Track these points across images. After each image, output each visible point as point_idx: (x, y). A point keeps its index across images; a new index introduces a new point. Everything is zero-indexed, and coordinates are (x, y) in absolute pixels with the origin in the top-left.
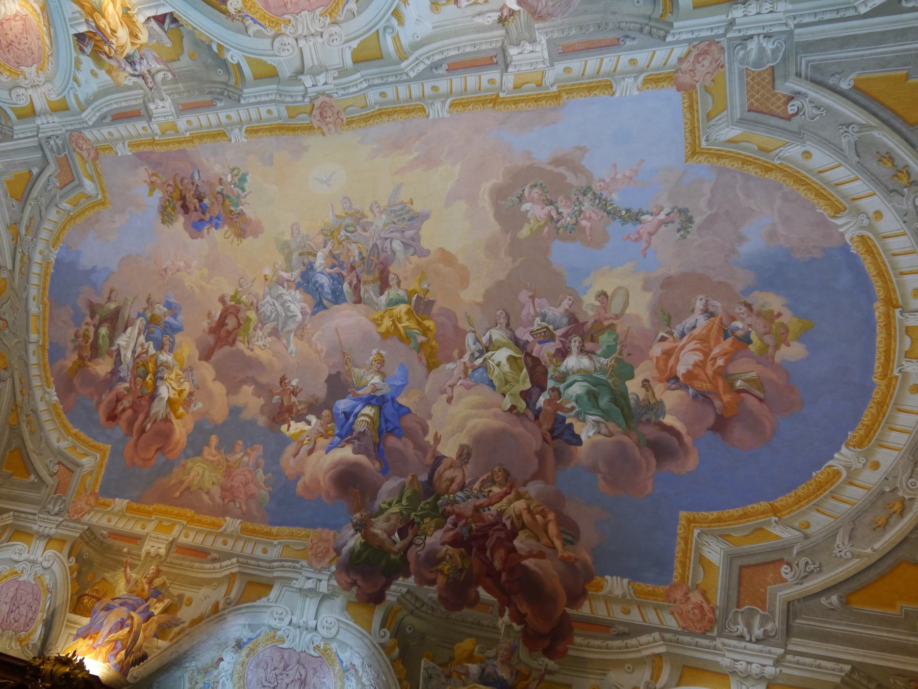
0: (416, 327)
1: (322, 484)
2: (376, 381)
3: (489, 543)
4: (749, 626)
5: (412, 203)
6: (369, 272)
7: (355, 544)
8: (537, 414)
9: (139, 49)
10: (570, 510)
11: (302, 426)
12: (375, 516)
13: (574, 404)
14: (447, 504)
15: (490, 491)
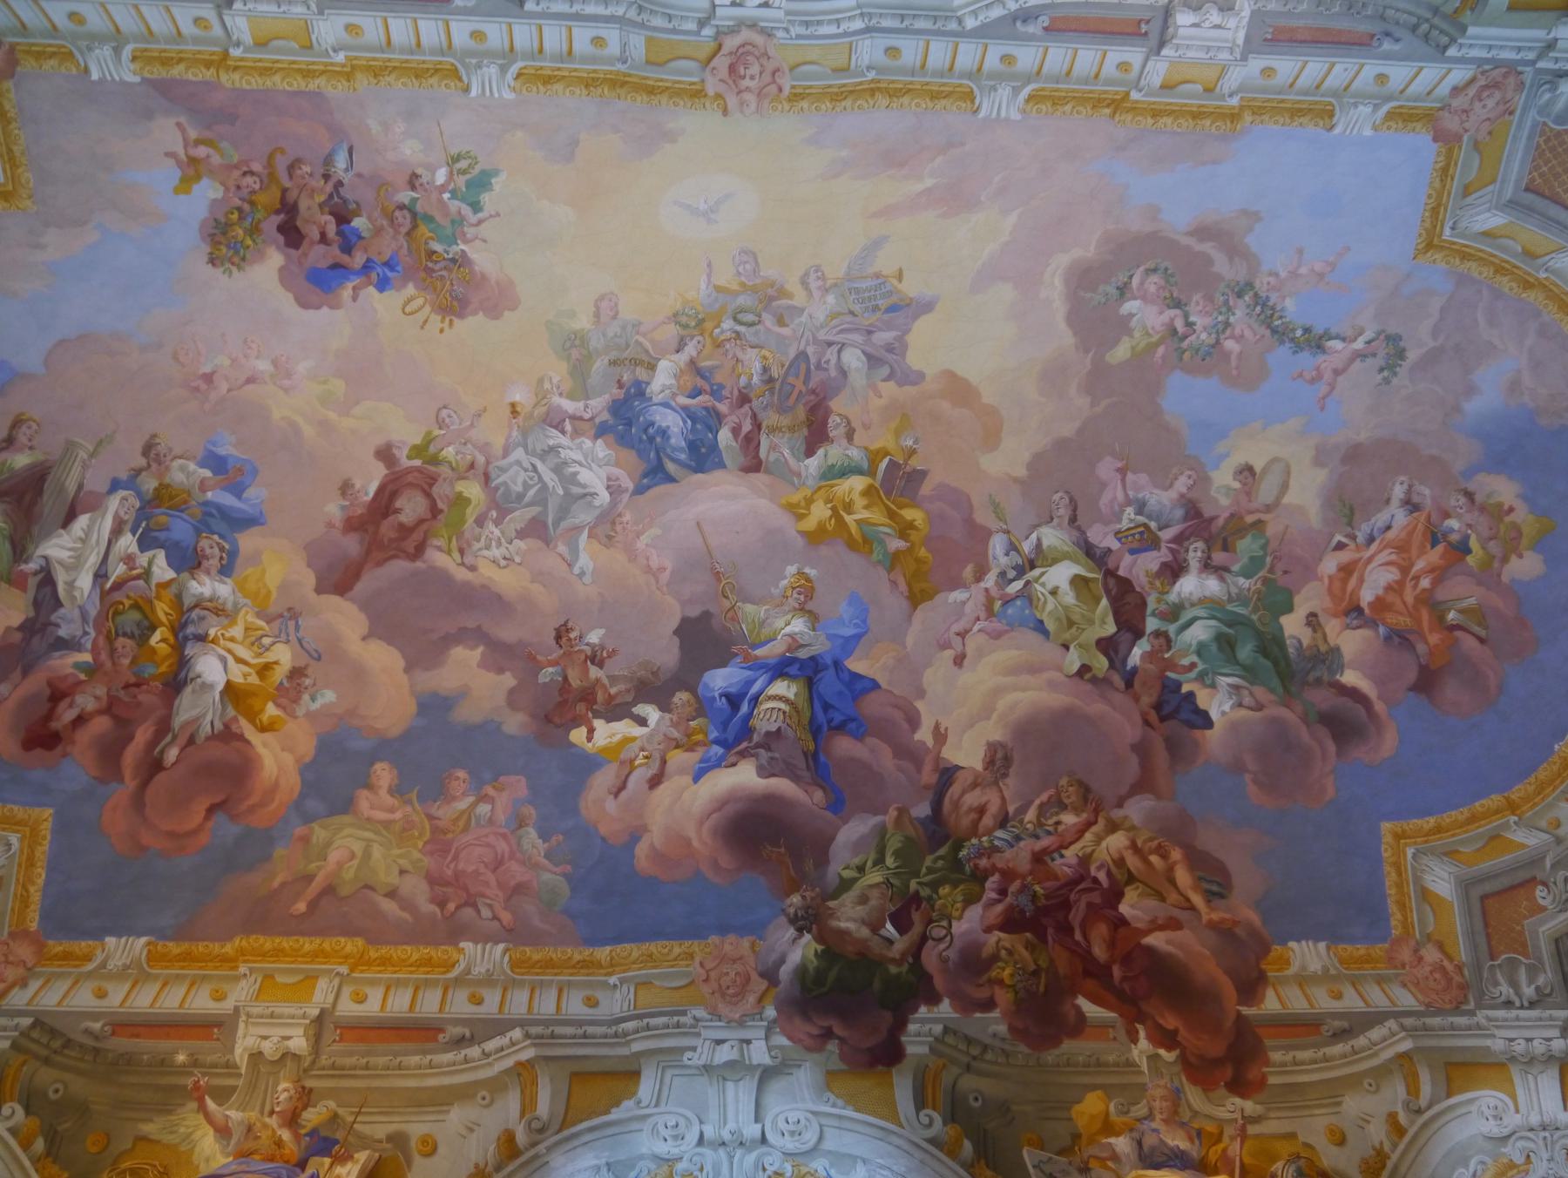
1: (695, 843)
2: (797, 630)
3: (1076, 916)
4: (1514, 984)
5: (900, 277)
6: (782, 410)
7: (804, 957)
8: (1130, 678)
10: (1207, 840)
11: (624, 728)
12: (835, 896)
13: (1195, 658)
14: (980, 855)
15: (1058, 823)
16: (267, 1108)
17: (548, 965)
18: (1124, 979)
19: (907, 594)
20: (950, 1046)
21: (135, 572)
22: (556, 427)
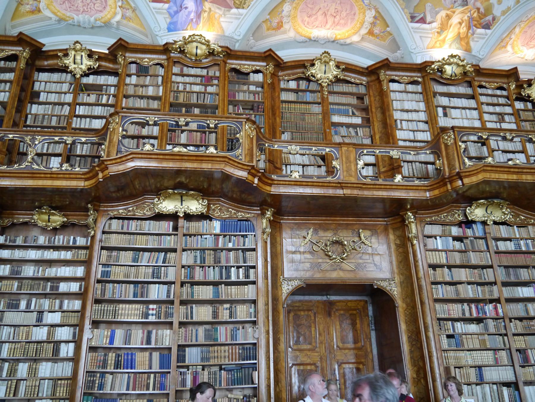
9: (452, 8)
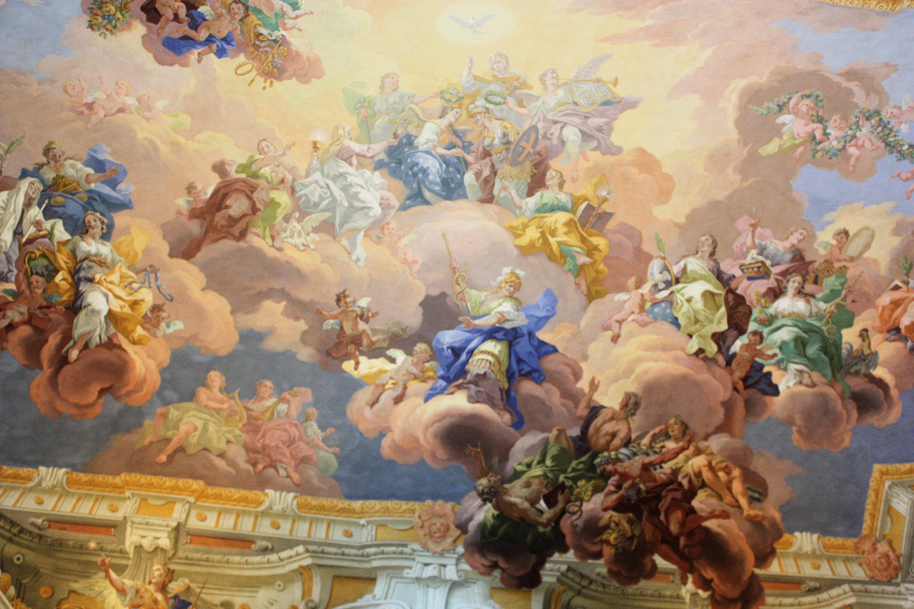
0: (579, 244)
1: (422, 441)
3: (663, 505)
5: (615, 83)
6: (514, 163)
7: (485, 517)
10: (759, 465)
11: (380, 363)
13: (777, 351)
14: (608, 463)
15: (663, 447)
16: (147, 580)
17: (321, 509)
18: (686, 546)
19: (585, 292)
20: (570, 579)
21: (42, 233)
22: (346, 160)
